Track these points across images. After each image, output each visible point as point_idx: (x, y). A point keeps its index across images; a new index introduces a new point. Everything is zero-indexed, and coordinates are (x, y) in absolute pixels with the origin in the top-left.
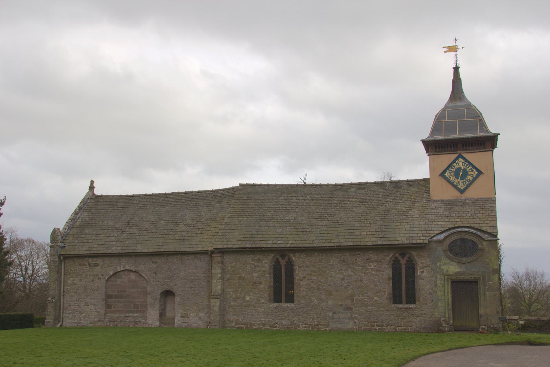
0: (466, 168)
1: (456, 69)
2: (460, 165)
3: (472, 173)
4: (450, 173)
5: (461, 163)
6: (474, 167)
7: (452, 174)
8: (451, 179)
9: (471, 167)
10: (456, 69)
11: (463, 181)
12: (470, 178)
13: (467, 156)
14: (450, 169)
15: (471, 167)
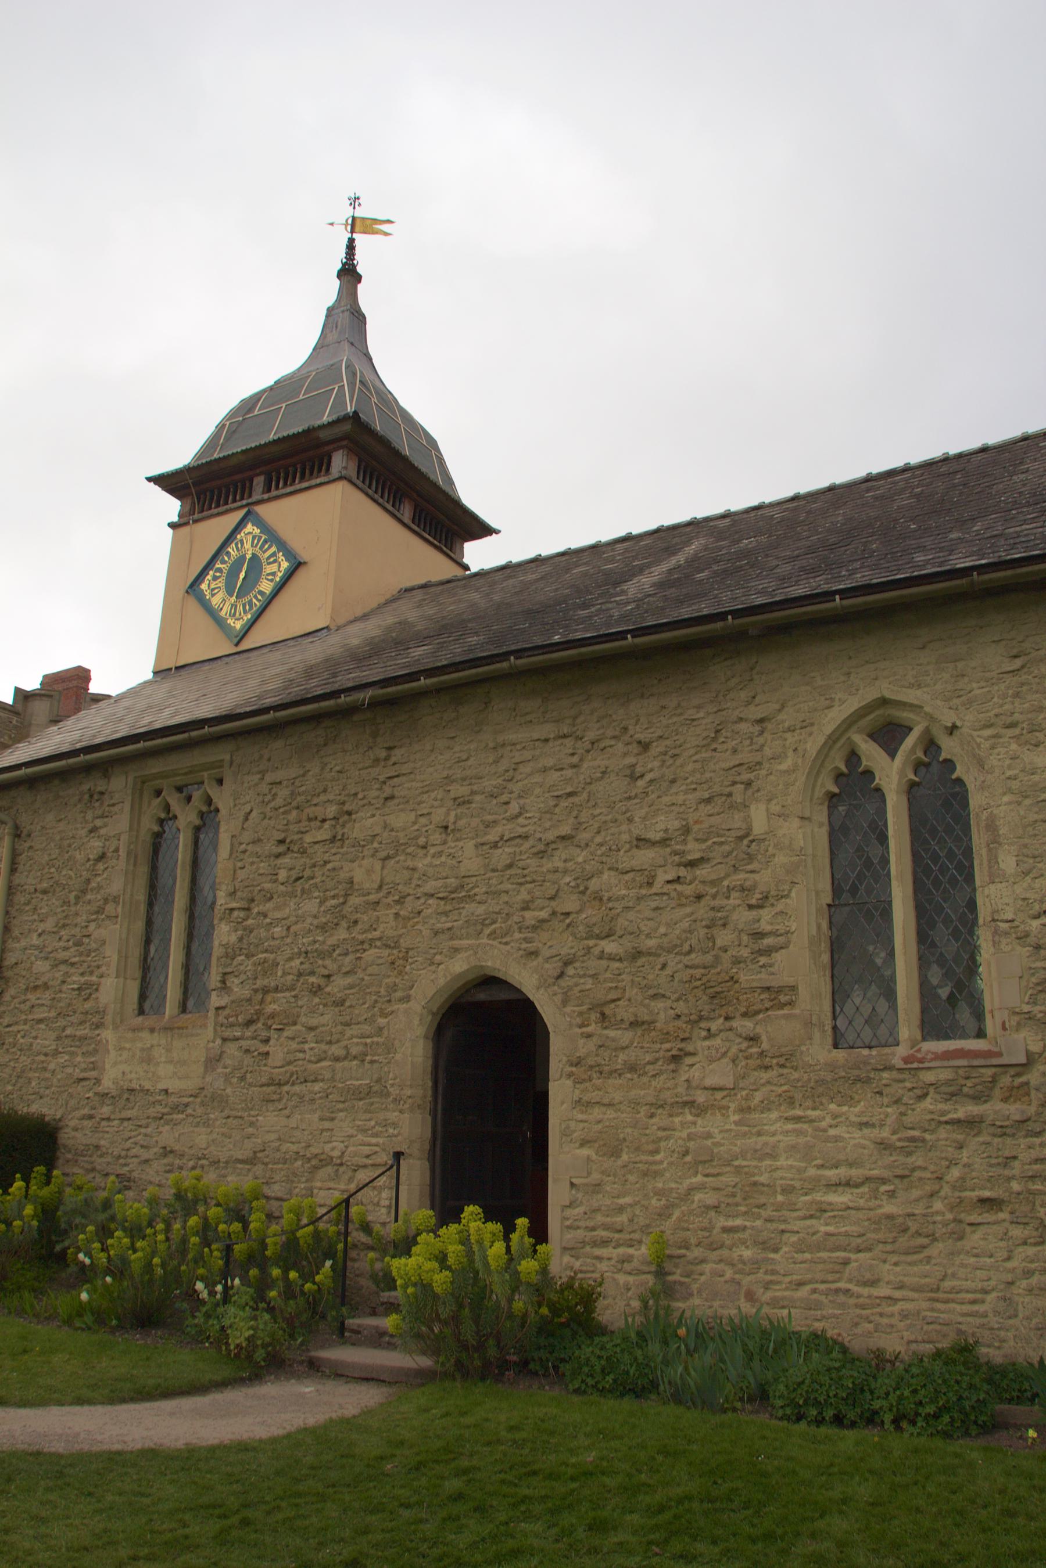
0: (259, 553)
1: (349, 274)
2: (248, 546)
3: (273, 568)
4: (215, 578)
5: (250, 538)
6: (283, 547)
7: (221, 583)
8: (215, 601)
9: (274, 549)
10: (349, 274)
11: (246, 599)
12: (266, 587)
13: (267, 511)
14: (218, 565)
15: (274, 549)
